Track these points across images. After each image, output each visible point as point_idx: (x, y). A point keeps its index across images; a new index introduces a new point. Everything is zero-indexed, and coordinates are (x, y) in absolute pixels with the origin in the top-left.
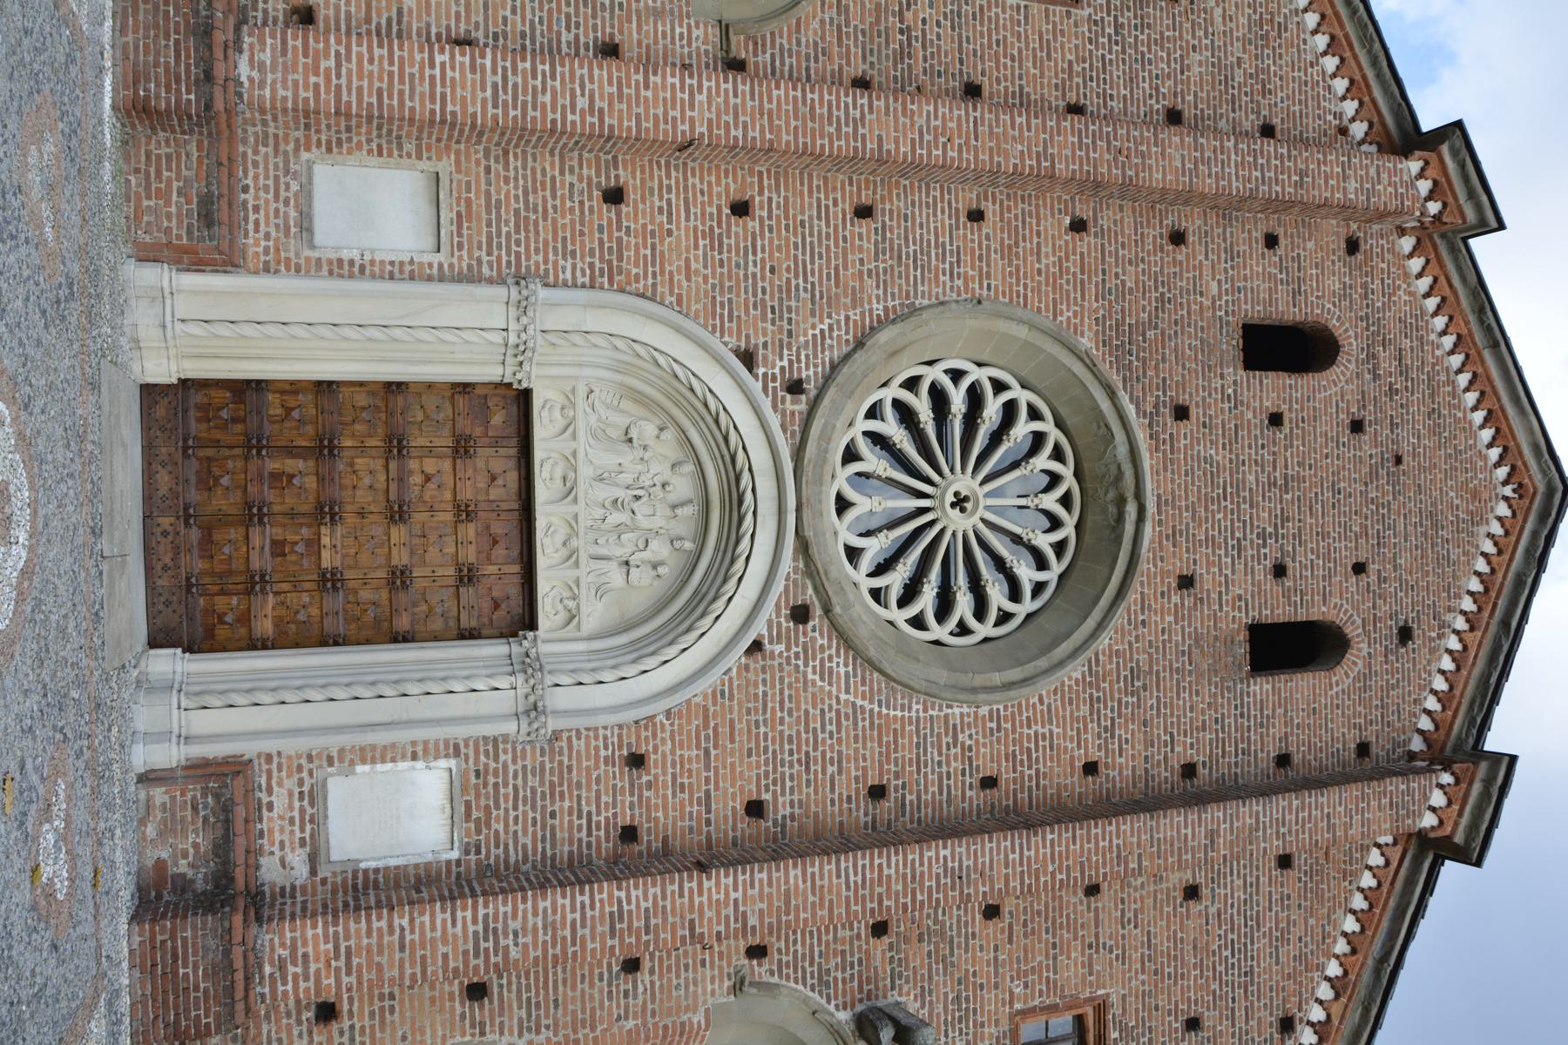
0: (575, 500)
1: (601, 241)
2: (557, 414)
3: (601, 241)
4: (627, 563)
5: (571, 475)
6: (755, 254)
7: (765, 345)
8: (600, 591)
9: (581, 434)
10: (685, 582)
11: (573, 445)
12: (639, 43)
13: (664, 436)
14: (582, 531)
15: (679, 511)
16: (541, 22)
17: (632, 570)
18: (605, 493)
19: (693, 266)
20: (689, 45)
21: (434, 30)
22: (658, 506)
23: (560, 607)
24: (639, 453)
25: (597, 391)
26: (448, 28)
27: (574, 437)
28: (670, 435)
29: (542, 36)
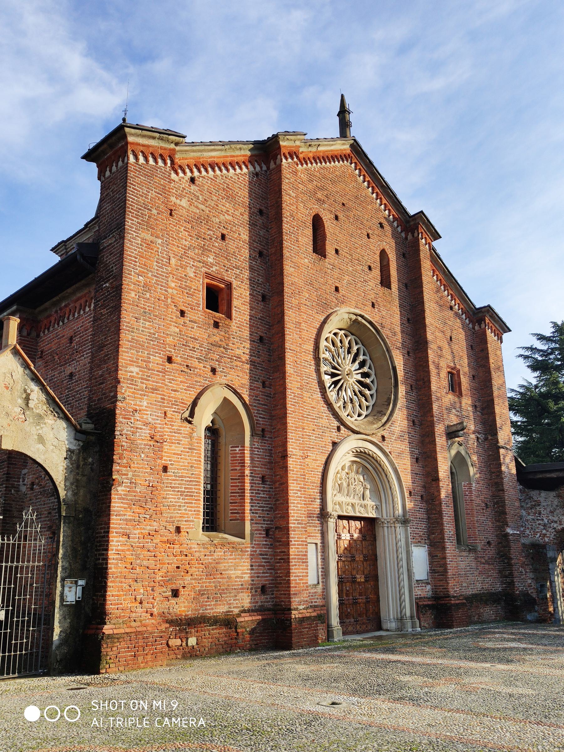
1: (311, 489)
3: (311, 489)
6: (310, 436)
7: (331, 437)
12: (261, 468)
16: (258, 503)
19: (314, 458)
20: (259, 449)
21: (264, 543)
26: (263, 537)
29: (262, 503)
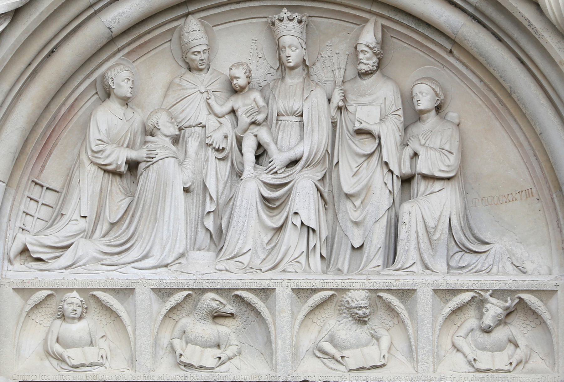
0: (265, 293)
2: (77, 329)
4: (407, 181)
5: (209, 300)
8: (466, 242)
9: (120, 277)
10: (454, 43)
11: (143, 296)
13: (123, 87)
14: (333, 280)
15: (293, 56)
17: (423, 167)
18: (248, 224)
22: (280, 105)
23: (501, 334)
24: (161, 145)
25: (23, 239)
27: (125, 292)
28: (120, 76)
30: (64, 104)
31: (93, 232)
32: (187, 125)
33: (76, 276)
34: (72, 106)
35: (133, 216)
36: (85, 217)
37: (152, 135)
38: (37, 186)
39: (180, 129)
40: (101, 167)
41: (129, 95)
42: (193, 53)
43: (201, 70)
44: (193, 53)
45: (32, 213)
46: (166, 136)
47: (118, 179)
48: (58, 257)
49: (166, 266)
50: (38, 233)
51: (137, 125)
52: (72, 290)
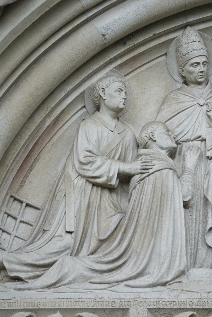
30: (48, 115)
31: (79, 251)
32: (184, 139)
33: (61, 296)
34: (57, 119)
35: (125, 232)
36: (71, 233)
37: (145, 147)
38: (16, 202)
39: (177, 143)
40: (88, 179)
41: (121, 106)
42: (192, 65)
43: (200, 83)
44: (192, 65)
45: (10, 230)
46: (162, 148)
47: (106, 193)
48: (39, 276)
49: (164, 284)
50: (18, 251)
51: (129, 139)
52: (54, 311)
